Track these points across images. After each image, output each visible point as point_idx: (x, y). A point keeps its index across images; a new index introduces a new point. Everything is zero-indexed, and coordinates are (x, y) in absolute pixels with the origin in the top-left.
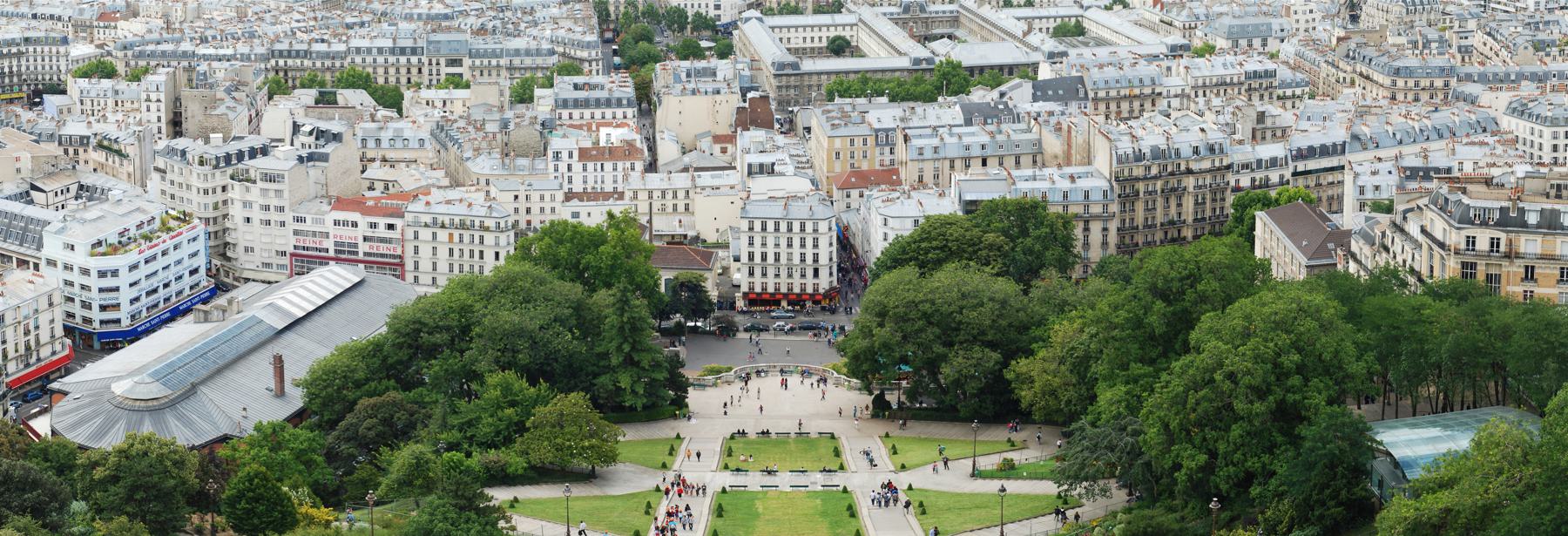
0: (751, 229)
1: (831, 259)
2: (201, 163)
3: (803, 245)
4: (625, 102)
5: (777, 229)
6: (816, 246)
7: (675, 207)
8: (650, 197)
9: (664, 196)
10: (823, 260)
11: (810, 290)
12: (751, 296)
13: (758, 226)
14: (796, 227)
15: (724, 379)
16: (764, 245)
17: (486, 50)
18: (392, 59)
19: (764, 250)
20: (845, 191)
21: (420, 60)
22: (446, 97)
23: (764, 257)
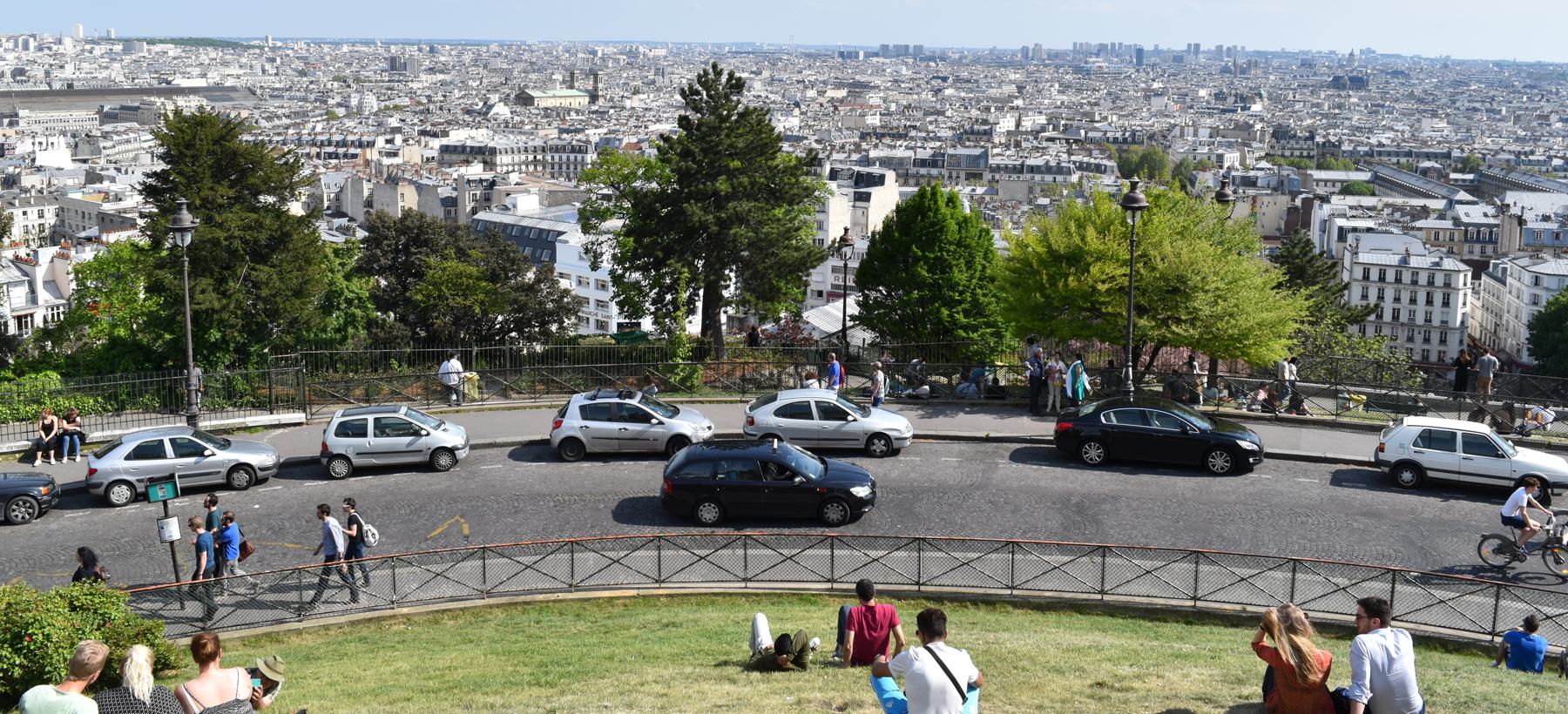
0: (1366, 277)
11: (1434, 358)
13: (1374, 275)
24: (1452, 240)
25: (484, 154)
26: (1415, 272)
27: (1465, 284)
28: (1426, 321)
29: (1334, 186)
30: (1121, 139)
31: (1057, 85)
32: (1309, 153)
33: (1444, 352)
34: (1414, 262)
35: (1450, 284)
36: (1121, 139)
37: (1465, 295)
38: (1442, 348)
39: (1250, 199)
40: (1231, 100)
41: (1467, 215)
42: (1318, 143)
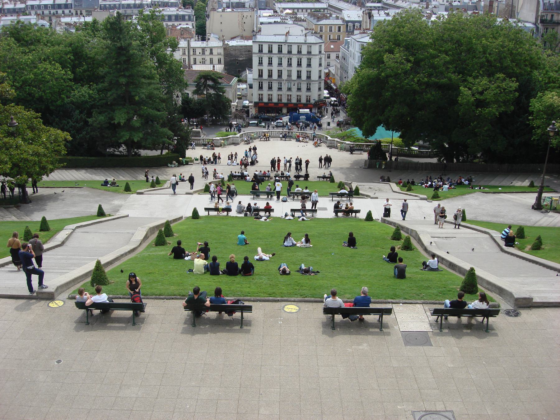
0: (261, 51)
1: (320, 77)
3: (299, 64)
4: (187, 18)
5: (280, 51)
6: (309, 65)
7: (211, 61)
9: (203, 53)
10: (315, 76)
12: (260, 104)
13: (265, 49)
14: (295, 50)
15: (230, 141)
16: (270, 64)
17: (110, 5)
18: (52, 11)
19: (270, 68)
20: (327, 53)
22: (78, 21)
23: (270, 75)
24: (339, 30)
26: (290, 45)
29: (307, 11)
34: (291, 39)
35: (311, 52)
37: (321, 59)
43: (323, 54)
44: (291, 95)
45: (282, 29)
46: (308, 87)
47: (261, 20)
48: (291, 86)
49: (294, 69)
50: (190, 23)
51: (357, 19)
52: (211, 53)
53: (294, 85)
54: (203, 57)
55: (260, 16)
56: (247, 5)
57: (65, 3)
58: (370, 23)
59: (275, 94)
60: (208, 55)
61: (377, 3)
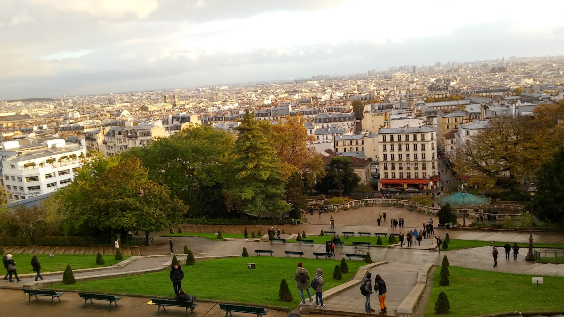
0: (384, 140)
1: (433, 158)
2: (120, 133)
3: (415, 149)
4: (347, 119)
6: (423, 149)
7: (357, 149)
8: (344, 145)
9: (351, 144)
10: (429, 157)
11: (420, 176)
13: (388, 138)
14: (411, 138)
16: (392, 149)
19: (392, 153)
20: (450, 139)
21: (269, 118)
23: (393, 157)
25: (79, 129)
27: (432, 139)
28: (415, 159)
30: (364, 98)
31: (373, 84)
32: (446, 96)
33: (425, 173)
35: (424, 139)
36: (364, 98)
37: (433, 144)
38: (424, 171)
39: (384, 114)
40: (443, 81)
41: (472, 109)
42: (450, 91)
43: (435, 140)
44: (410, 173)
45: (402, 123)
46: (423, 166)
47: (392, 117)
48: (409, 166)
49: (412, 152)
50: (350, 123)
51: (479, 111)
52: (357, 144)
53: (412, 165)
54: (351, 147)
55: (392, 115)
56: (394, 107)
57: (266, 112)
58: (486, 113)
59: (397, 172)
60: (354, 145)
61: (517, 95)
